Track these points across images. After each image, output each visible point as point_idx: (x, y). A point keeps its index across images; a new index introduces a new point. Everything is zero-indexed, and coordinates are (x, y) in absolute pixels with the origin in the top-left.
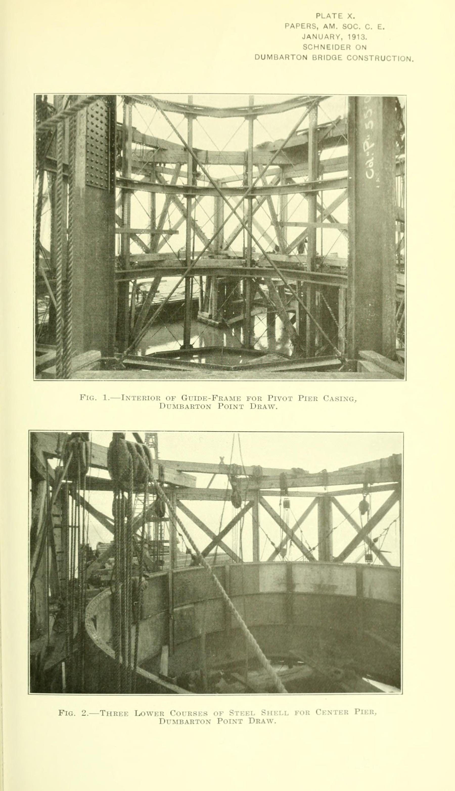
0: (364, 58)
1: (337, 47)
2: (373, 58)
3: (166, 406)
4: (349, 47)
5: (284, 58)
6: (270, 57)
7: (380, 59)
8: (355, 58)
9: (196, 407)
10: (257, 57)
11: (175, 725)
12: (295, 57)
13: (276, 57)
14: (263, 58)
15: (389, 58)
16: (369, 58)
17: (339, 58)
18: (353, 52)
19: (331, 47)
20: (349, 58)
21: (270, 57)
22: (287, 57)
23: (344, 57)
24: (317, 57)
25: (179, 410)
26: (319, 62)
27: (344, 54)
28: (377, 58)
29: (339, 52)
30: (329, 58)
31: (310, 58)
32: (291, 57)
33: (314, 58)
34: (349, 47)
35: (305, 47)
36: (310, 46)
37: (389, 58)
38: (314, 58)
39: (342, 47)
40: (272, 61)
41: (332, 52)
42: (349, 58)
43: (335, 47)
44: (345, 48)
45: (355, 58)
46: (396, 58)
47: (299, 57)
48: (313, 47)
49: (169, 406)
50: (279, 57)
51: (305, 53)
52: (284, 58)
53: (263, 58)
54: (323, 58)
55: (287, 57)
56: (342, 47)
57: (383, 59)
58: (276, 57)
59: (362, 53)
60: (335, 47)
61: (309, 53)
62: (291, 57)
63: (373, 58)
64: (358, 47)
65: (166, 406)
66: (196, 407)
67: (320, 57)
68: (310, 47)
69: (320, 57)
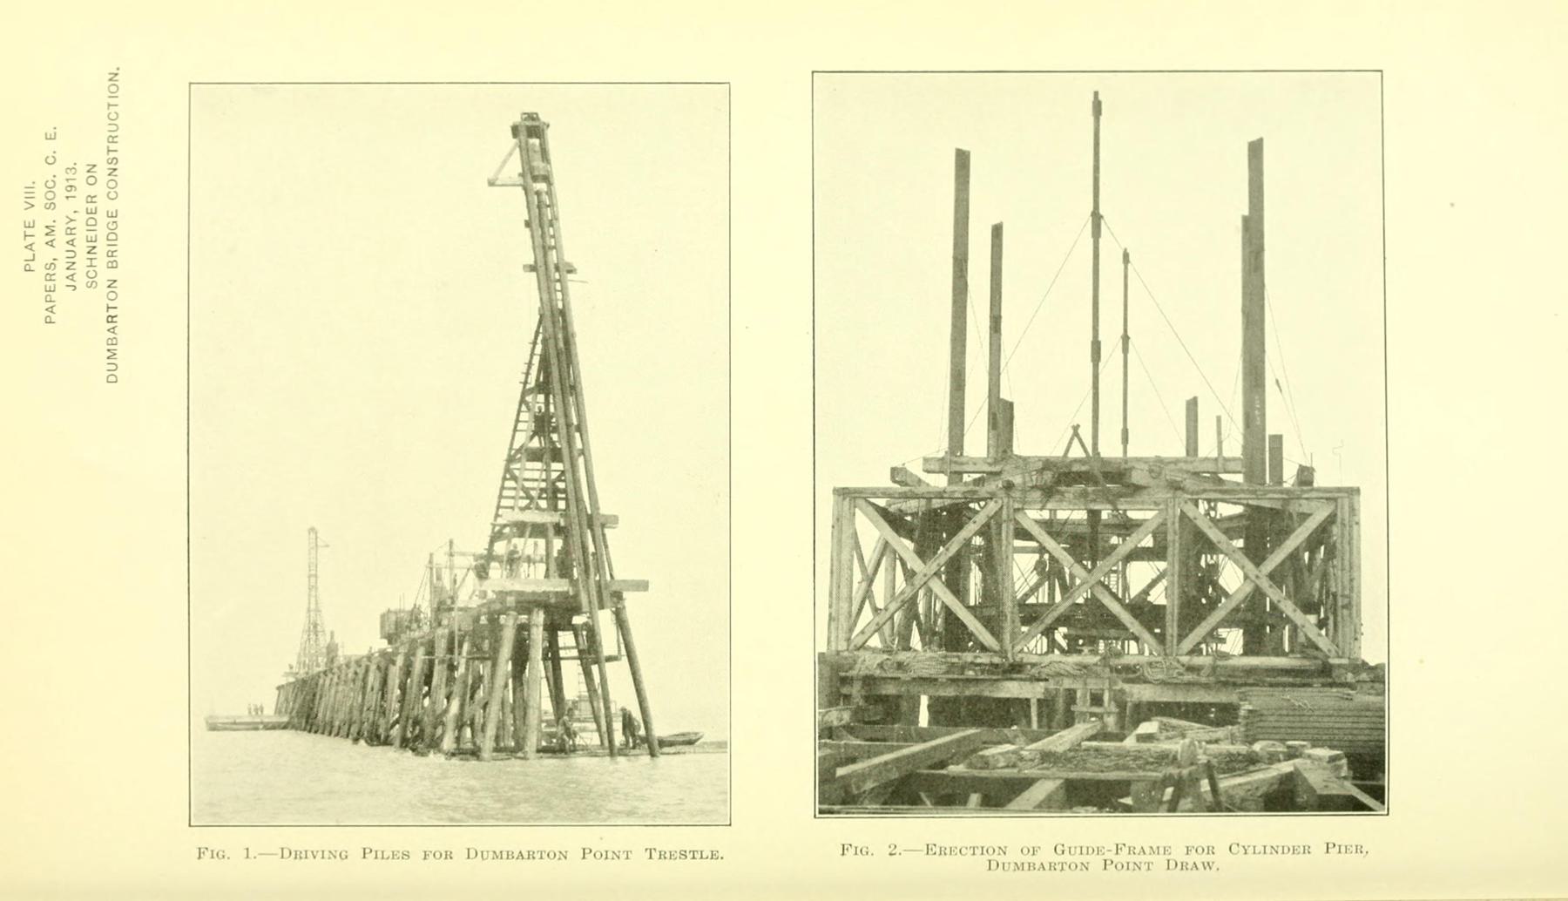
2: (112, 147)
4: (91, 199)
6: (112, 355)
8: (112, 184)
10: (112, 379)
13: (113, 342)
15: (113, 116)
16: (112, 155)
17: (113, 215)
18: (100, 190)
20: (113, 195)
21: (112, 355)
22: (111, 319)
23: (112, 206)
26: (119, 257)
27: (103, 205)
28: (112, 139)
29: (101, 217)
30: (112, 237)
31: (112, 274)
32: (112, 312)
33: (113, 265)
34: (91, 199)
35: (92, 284)
36: (92, 274)
37: (113, 116)
39: (91, 213)
40: (120, 350)
41: (102, 231)
42: (113, 195)
43: (91, 226)
44: (91, 206)
45: (112, 184)
47: (112, 296)
51: (102, 281)
55: (111, 319)
56: (91, 213)
58: (113, 342)
59: (102, 172)
60: (91, 226)
61: (104, 275)
62: (112, 312)
64: (92, 180)
67: (111, 254)
68: (92, 274)
69: (111, 254)
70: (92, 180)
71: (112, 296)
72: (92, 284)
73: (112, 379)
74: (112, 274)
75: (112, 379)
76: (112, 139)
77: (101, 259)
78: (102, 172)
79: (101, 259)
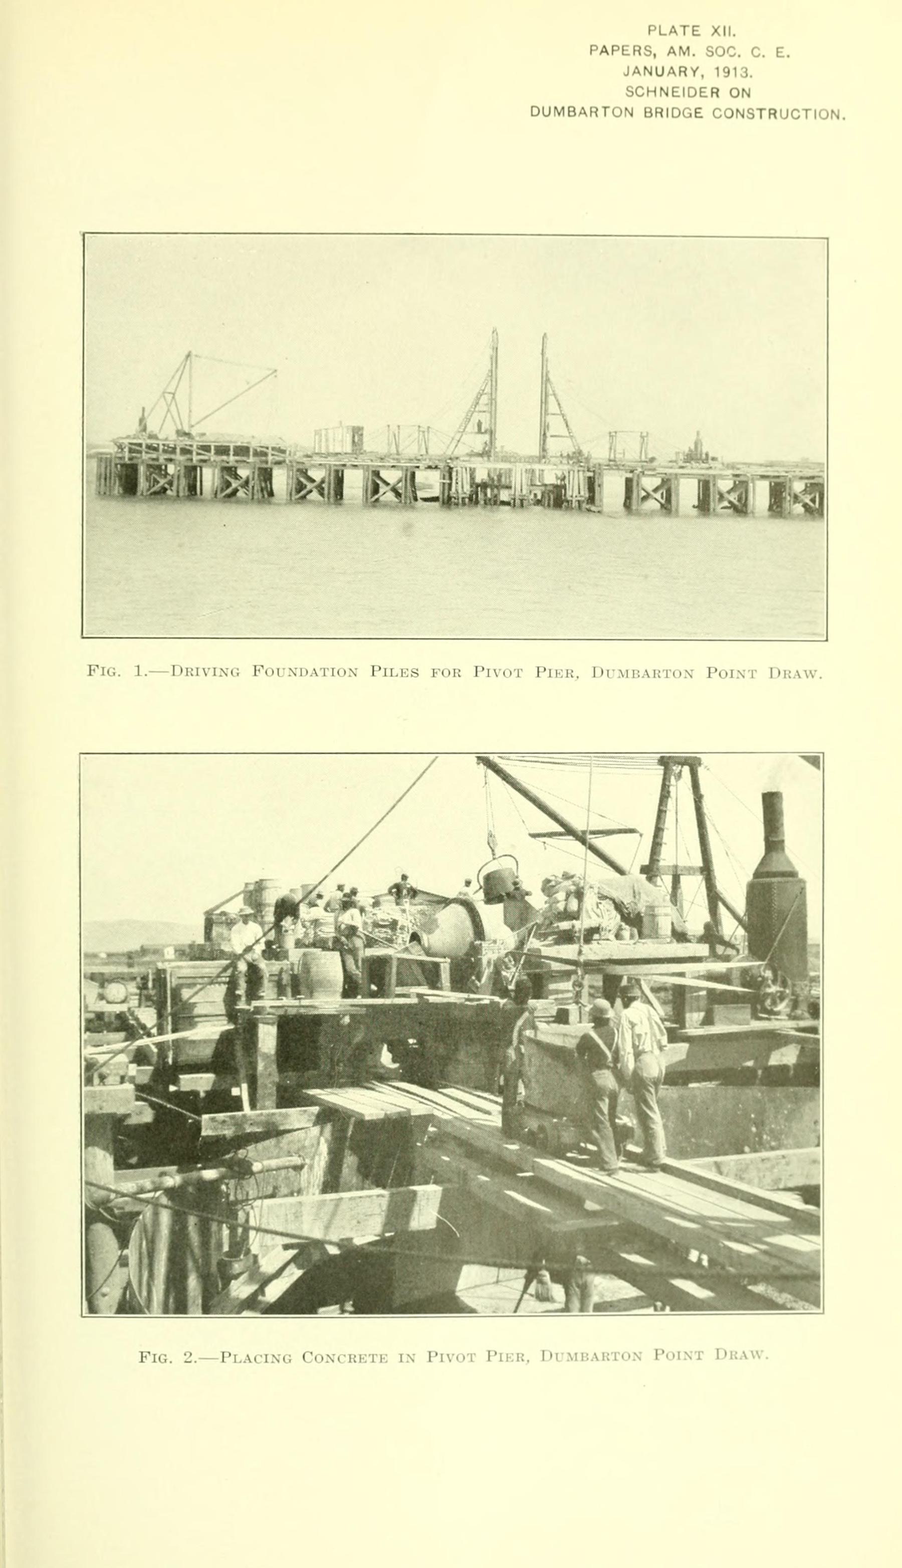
0: (746, 113)
1: (692, 92)
2: (765, 114)
3: (605, 672)
5: (588, 112)
6: (559, 112)
7: (778, 115)
8: (729, 113)
9: (663, 675)
10: (535, 111)
11: (571, 1363)
12: (609, 111)
14: (546, 113)
15: (796, 114)
16: (757, 113)
18: (725, 101)
19: (680, 93)
21: (559, 112)
22: (594, 111)
23: (706, 112)
24: (653, 112)
25: (630, 680)
27: (708, 104)
28: (773, 113)
29: (696, 102)
30: (676, 113)
32: (601, 112)
33: (648, 113)
34: (715, 92)
35: (631, 92)
38: (648, 113)
40: (565, 119)
41: (682, 103)
42: (717, 113)
43: (690, 92)
44: (708, 93)
46: (811, 114)
47: (617, 112)
48: (645, 91)
49: (611, 673)
50: (578, 111)
52: (588, 112)
53: (546, 113)
54: (664, 113)
55: (594, 111)
57: (784, 115)
59: (742, 103)
60: (690, 92)
61: (638, 104)
62: (601, 112)
63: (765, 114)
64: (735, 93)
65: (605, 672)
66: (663, 675)
68: (640, 92)
70: (735, 93)
71: (617, 112)
72: (631, 92)
73: (536, 111)
74: (639, 112)
75: (536, 111)
76: (773, 113)
77: (654, 102)
78: (742, 103)
79: (654, 102)
